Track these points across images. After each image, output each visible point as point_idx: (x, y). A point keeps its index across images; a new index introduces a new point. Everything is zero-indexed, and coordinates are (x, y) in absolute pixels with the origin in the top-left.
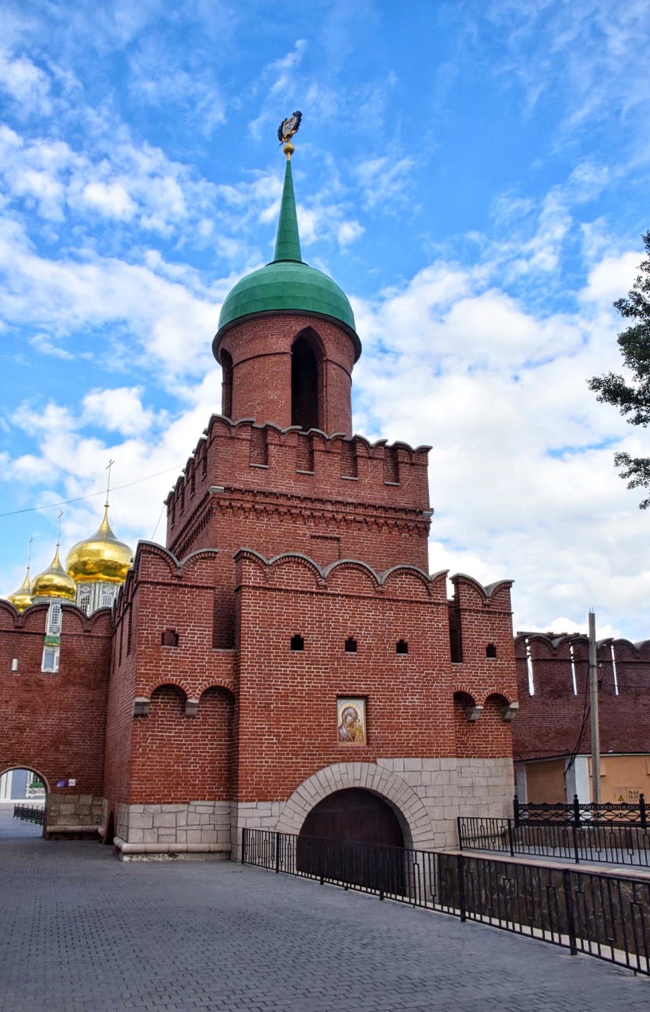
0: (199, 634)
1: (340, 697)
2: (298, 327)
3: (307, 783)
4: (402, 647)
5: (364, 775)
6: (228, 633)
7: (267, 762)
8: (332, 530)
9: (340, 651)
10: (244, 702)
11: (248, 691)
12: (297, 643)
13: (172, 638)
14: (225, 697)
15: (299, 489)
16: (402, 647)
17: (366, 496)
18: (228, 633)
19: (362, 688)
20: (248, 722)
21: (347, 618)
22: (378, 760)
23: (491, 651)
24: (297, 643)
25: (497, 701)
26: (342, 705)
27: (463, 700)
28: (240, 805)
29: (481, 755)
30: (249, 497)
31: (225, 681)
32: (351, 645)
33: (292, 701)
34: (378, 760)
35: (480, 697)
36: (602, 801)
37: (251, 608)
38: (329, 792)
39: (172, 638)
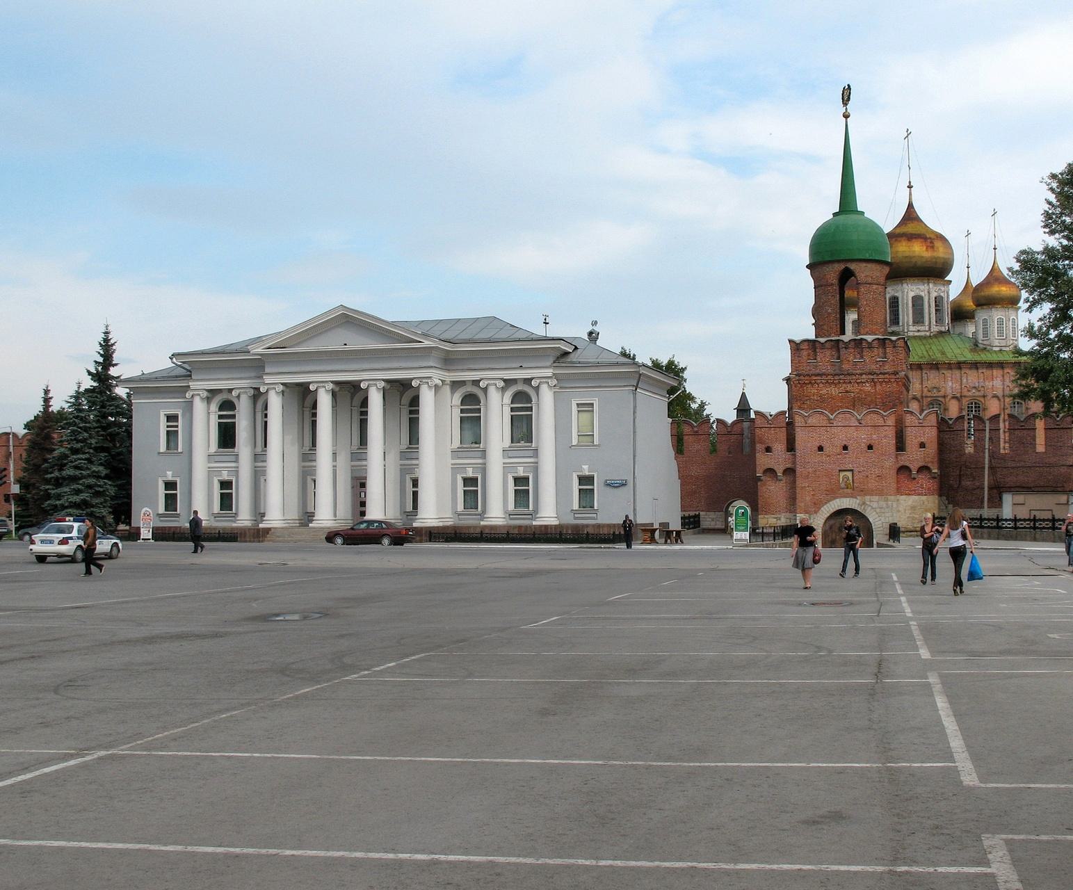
0: (779, 447)
1: (840, 471)
2: (839, 267)
3: (825, 506)
4: (870, 447)
5: (851, 503)
6: (791, 447)
10: (798, 474)
11: (799, 470)
12: (821, 449)
14: (790, 472)
16: (870, 447)
18: (791, 447)
19: (850, 467)
20: (800, 483)
22: (858, 497)
24: (821, 449)
25: (924, 469)
26: (842, 474)
27: (903, 469)
28: (798, 515)
30: (807, 378)
31: (789, 466)
33: (818, 473)
34: (858, 497)
35: (914, 467)
36: (1018, 518)
37: (800, 435)
38: (835, 510)
39: (768, 449)
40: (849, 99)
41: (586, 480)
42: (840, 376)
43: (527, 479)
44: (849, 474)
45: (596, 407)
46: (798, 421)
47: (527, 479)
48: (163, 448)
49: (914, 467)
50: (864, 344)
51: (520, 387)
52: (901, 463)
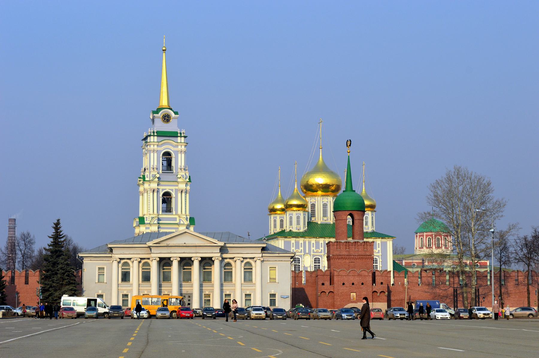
0: (327, 283)
4: (362, 284)
6: (331, 282)
7: (339, 303)
8: (353, 261)
9: (351, 285)
12: (344, 284)
13: (323, 284)
15: (346, 253)
16: (362, 284)
17: (360, 253)
18: (331, 282)
21: (352, 280)
23: (382, 283)
24: (344, 284)
26: (352, 294)
29: (380, 302)
32: (353, 284)
37: (336, 279)
39: (323, 284)
40: (350, 145)
41: (273, 295)
42: (348, 257)
43: (250, 295)
44: (355, 294)
45: (277, 268)
46: (336, 273)
47: (250, 295)
48: (97, 282)
49: (379, 292)
50: (359, 244)
51: (248, 260)
52: (374, 290)
